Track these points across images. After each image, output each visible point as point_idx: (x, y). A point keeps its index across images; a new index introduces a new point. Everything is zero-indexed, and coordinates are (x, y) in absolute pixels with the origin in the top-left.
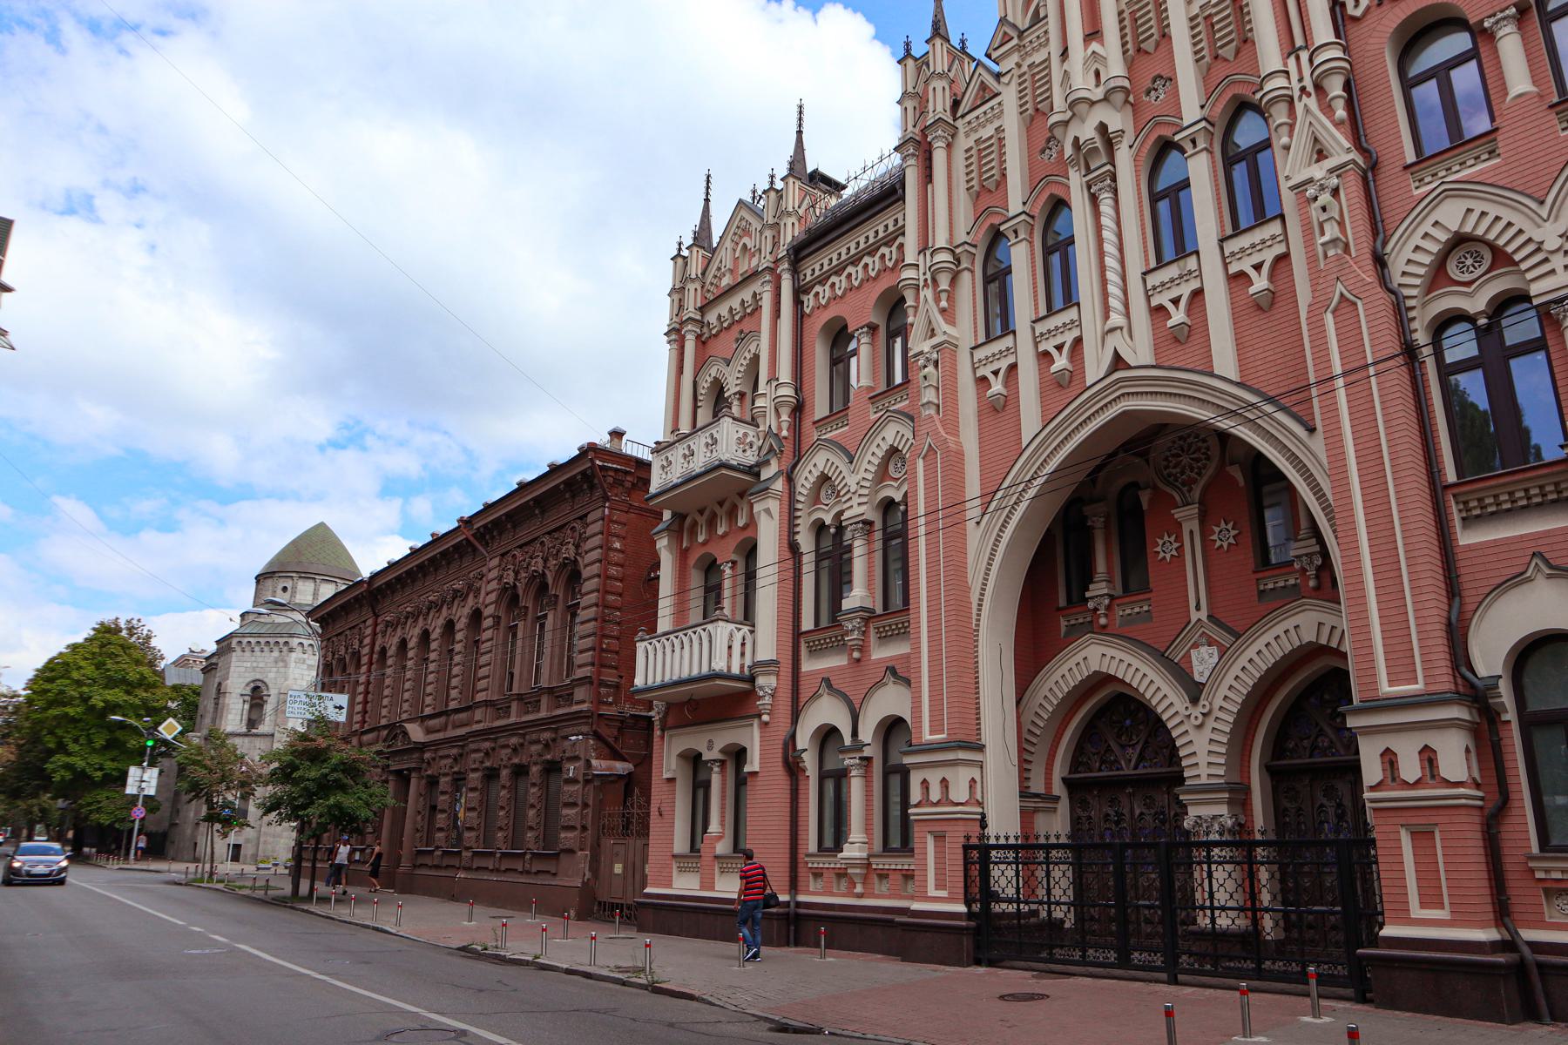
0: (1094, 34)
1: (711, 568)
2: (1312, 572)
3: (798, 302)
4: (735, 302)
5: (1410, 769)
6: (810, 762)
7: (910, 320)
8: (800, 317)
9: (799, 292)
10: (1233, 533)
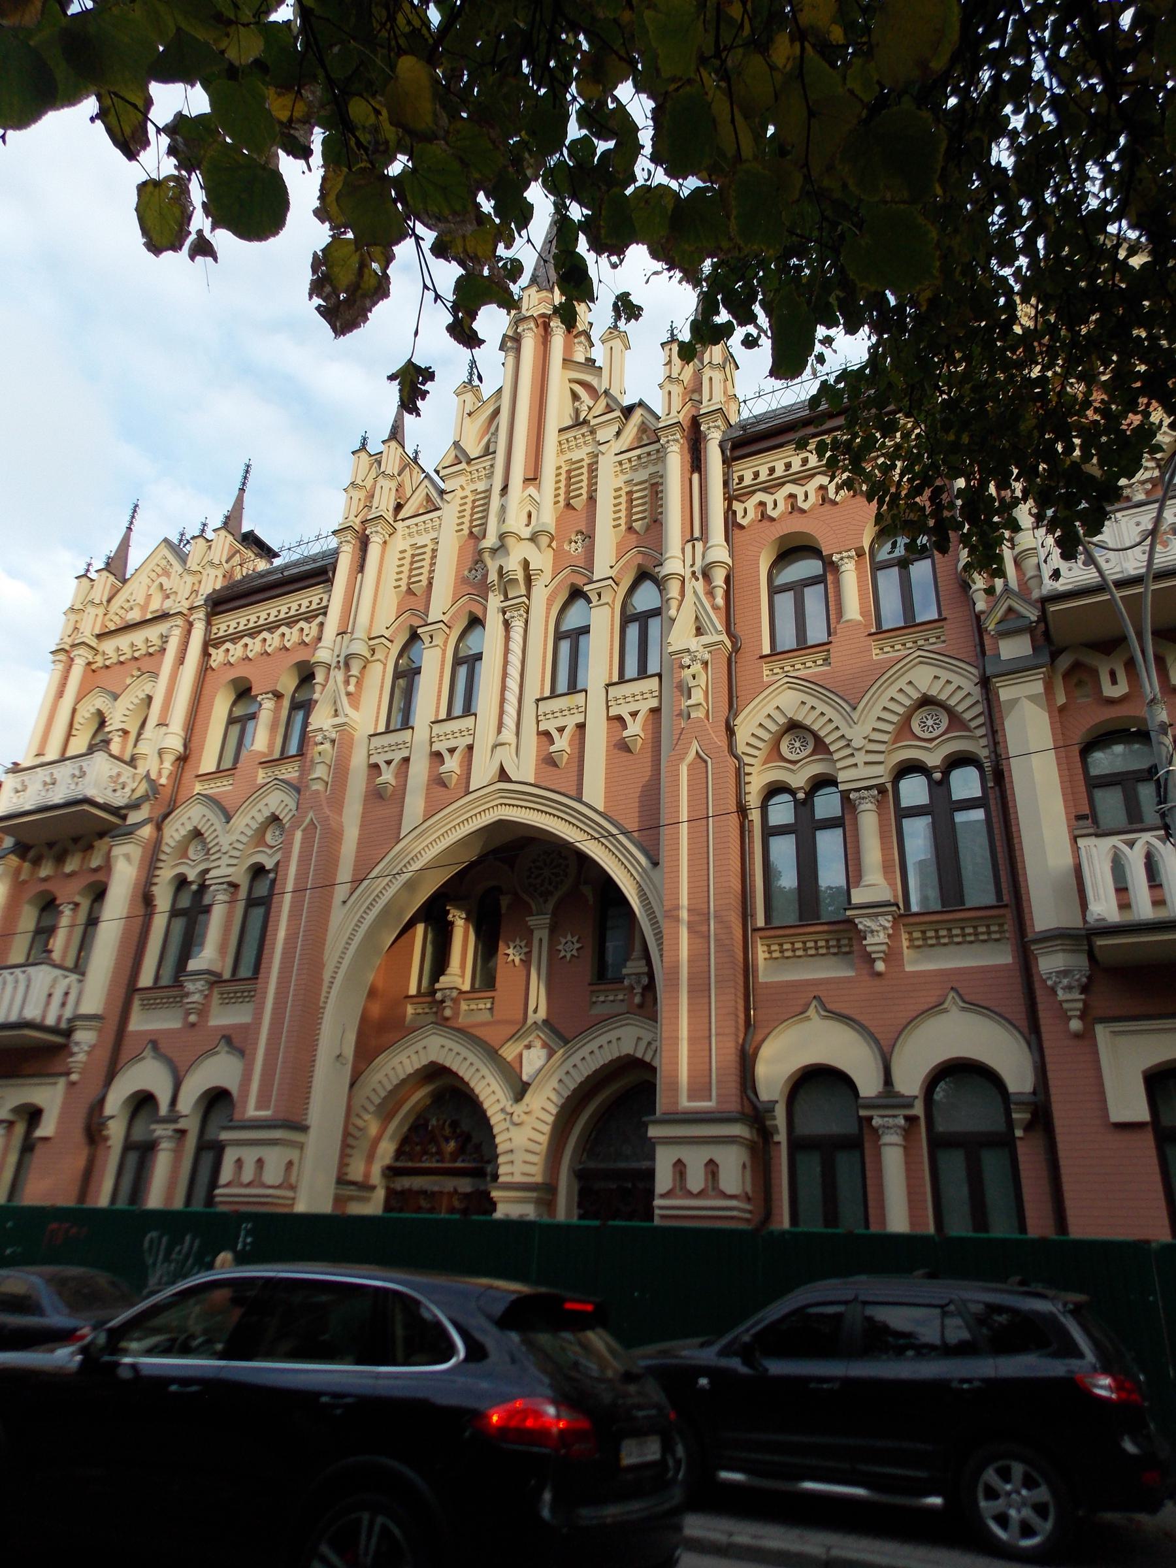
0: (533, 479)
1: (49, 906)
2: (638, 990)
3: (206, 654)
4: (138, 637)
5: (696, 1180)
6: (116, 1131)
7: (316, 696)
8: (205, 669)
9: (209, 644)
10: (577, 946)
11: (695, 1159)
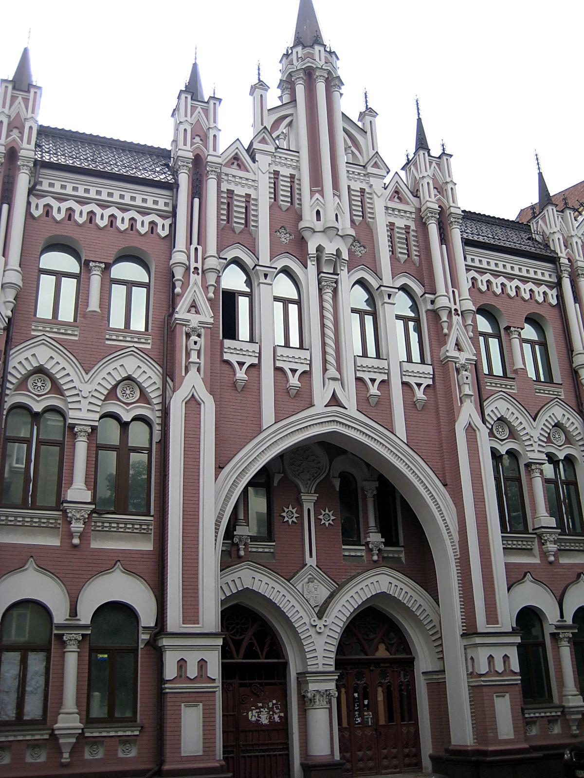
5: (499, 667)
10: (333, 518)
11: (498, 654)
